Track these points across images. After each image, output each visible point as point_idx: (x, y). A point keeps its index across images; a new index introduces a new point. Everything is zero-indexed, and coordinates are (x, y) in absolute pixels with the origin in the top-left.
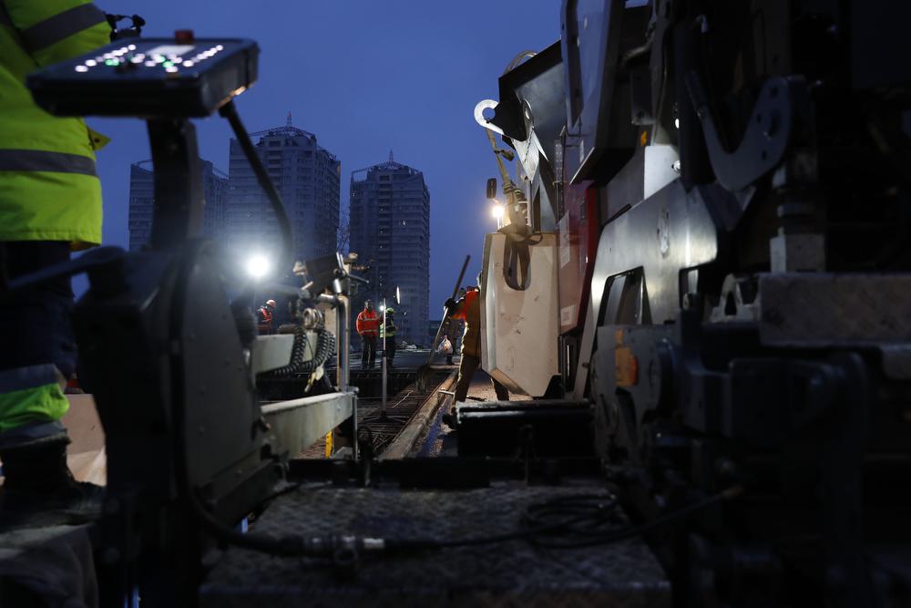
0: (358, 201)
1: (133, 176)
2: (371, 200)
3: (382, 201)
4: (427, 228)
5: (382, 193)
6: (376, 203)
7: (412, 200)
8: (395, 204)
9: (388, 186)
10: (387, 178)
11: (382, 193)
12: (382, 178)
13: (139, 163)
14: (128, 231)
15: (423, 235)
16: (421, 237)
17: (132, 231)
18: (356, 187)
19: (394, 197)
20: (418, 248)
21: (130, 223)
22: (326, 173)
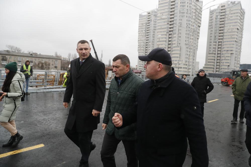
0: (211, 17)
1: (140, 17)
2: (217, 16)
3: (221, 16)
4: (243, 25)
5: (222, 13)
6: (219, 17)
7: (234, 13)
8: (227, 16)
9: (224, 9)
10: (224, 6)
11: (222, 13)
12: (222, 7)
13: (142, 13)
14: (138, 34)
15: (239, 28)
16: (238, 29)
17: (139, 34)
18: (212, 12)
19: (227, 13)
20: (237, 34)
21: (139, 31)
22: (194, 4)
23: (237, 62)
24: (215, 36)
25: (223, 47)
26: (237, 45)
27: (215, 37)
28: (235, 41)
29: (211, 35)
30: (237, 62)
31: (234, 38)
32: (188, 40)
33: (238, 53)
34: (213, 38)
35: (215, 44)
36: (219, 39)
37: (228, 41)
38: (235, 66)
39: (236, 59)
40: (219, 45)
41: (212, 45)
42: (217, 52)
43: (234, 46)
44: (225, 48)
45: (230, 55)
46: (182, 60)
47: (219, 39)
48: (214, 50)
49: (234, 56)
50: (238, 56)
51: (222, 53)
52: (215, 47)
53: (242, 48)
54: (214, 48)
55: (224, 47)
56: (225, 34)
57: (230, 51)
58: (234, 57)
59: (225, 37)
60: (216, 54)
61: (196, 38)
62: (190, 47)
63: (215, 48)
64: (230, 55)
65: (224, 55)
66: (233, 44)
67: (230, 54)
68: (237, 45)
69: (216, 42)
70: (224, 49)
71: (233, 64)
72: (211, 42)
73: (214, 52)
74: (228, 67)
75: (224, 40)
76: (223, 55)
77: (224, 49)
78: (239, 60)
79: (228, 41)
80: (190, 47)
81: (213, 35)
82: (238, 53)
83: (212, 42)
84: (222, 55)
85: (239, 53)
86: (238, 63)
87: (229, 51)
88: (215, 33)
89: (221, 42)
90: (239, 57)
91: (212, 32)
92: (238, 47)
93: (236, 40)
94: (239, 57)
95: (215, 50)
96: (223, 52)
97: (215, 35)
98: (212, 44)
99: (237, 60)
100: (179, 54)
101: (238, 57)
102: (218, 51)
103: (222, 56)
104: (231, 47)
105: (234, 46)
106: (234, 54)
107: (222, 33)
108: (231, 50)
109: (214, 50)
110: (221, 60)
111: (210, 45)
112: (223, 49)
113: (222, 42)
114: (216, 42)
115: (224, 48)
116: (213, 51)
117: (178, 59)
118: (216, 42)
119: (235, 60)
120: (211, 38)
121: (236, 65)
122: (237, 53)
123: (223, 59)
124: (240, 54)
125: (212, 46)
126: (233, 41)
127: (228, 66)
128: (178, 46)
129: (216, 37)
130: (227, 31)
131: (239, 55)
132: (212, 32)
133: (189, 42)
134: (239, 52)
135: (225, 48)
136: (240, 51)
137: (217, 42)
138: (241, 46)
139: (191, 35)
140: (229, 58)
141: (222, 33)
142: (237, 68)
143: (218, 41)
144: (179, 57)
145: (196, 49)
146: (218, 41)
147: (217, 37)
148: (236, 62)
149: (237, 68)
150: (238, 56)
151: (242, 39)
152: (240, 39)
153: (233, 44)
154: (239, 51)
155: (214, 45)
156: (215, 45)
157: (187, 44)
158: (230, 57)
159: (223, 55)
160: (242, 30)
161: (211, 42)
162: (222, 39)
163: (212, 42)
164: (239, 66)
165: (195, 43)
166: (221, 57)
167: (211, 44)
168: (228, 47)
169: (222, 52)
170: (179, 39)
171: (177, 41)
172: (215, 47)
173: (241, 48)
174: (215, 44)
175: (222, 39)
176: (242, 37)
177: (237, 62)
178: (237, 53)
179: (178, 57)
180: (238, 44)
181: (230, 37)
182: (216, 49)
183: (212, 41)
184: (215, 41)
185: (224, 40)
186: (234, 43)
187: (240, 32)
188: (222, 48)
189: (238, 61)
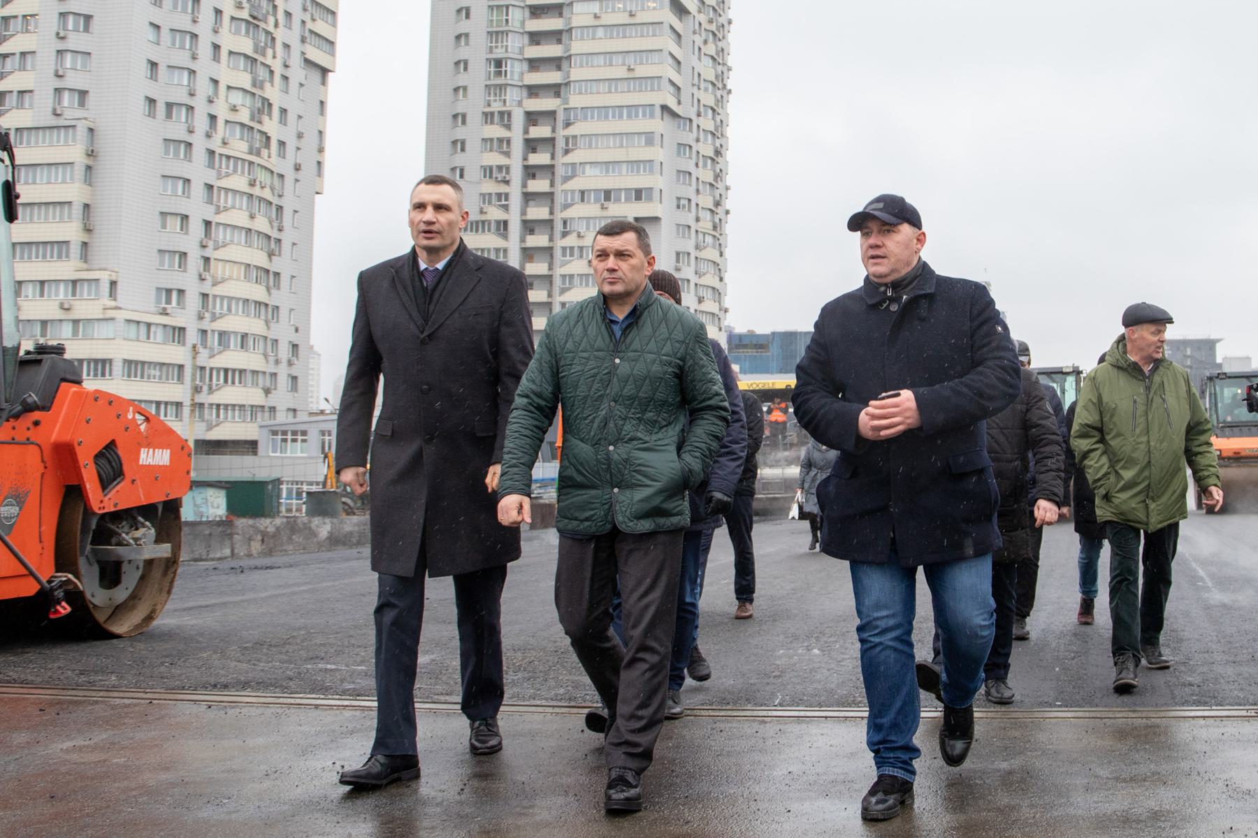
20: (673, 47)
24: (498, 63)
25: (570, 158)
26: (682, 147)
27: (499, 74)
28: (665, 108)
29: (463, 53)
31: (652, 81)
32: (183, 58)
34: (477, 77)
35: (496, 131)
36: (533, 91)
37: (604, 112)
40: (532, 145)
41: (473, 145)
42: (524, 213)
43: (657, 153)
44: (589, 170)
46: (105, 277)
47: (533, 91)
48: (491, 187)
51: (559, 216)
52: (494, 159)
54: (488, 171)
55: (573, 164)
56: (577, 47)
57: (628, 200)
59: (576, 73)
60: (515, 228)
61: (296, 60)
62: (208, 136)
63: (500, 168)
65: (579, 236)
66: (649, 138)
68: (682, 147)
69: (509, 114)
70: (576, 184)
72: (460, 118)
73: (495, 214)
75: (576, 101)
76: (571, 241)
77: (576, 184)
79: (604, 112)
80: (215, 144)
81: (477, 52)
82: (698, 220)
83: (475, 118)
84: (565, 234)
85: (706, 225)
87: (618, 200)
88: (496, 35)
89: (552, 114)
91: (464, 26)
92: (692, 169)
93: (672, 104)
95: (503, 189)
96: (568, 214)
97: (499, 53)
98: (476, 131)
100: (77, 210)
101: (702, 254)
102: (528, 197)
103: (560, 243)
104: (635, 164)
105: (657, 153)
107: (556, 36)
108: (638, 194)
109: (491, 187)
110: (557, 282)
111: (454, 142)
112: (566, 179)
113: (561, 117)
114: (505, 118)
115: (574, 171)
116: (487, 198)
117: (67, 269)
118: (501, 114)
120: (462, 79)
122: (693, 214)
123: (571, 276)
125: (476, 159)
128: (59, 128)
129: (510, 67)
130: (590, 21)
131: (709, 239)
132: (464, 26)
133: (204, 88)
135: (589, 170)
137: (518, 119)
139: (226, 18)
141: (556, 36)
143: (520, 104)
144: (75, 249)
145: (297, 168)
146: (520, 104)
147: (516, 72)
150: (697, 247)
151: (720, 101)
152: (708, 99)
153: (649, 138)
154: (706, 201)
155: (492, 140)
156: (503, 145)
157: (169, 106)
159: (571, 241)
160: (713, 27)
161: (460, 118)
162: (555, 90)
163: (475, 118)
165: (284, 111)
166: (558, 253)
167: (460, 133)
168: (607, 165)
169: (566, 207)
170: (76, 41)
171: (46, 61)
172: (494, 159)
173: (717, 177)
174: (496, 131)
175: (555, 90)
176: (719, 84)
177: (700, 300)
178: (689, 219)
179: (61, 246)
181: (621, 72)
182: (507, 182)
183: (474, 104)
184: (496, 107)
185: (576, 101)
186: (658, 125)
187: (699, 40)
188: (560, 172)
189: (708, 294)
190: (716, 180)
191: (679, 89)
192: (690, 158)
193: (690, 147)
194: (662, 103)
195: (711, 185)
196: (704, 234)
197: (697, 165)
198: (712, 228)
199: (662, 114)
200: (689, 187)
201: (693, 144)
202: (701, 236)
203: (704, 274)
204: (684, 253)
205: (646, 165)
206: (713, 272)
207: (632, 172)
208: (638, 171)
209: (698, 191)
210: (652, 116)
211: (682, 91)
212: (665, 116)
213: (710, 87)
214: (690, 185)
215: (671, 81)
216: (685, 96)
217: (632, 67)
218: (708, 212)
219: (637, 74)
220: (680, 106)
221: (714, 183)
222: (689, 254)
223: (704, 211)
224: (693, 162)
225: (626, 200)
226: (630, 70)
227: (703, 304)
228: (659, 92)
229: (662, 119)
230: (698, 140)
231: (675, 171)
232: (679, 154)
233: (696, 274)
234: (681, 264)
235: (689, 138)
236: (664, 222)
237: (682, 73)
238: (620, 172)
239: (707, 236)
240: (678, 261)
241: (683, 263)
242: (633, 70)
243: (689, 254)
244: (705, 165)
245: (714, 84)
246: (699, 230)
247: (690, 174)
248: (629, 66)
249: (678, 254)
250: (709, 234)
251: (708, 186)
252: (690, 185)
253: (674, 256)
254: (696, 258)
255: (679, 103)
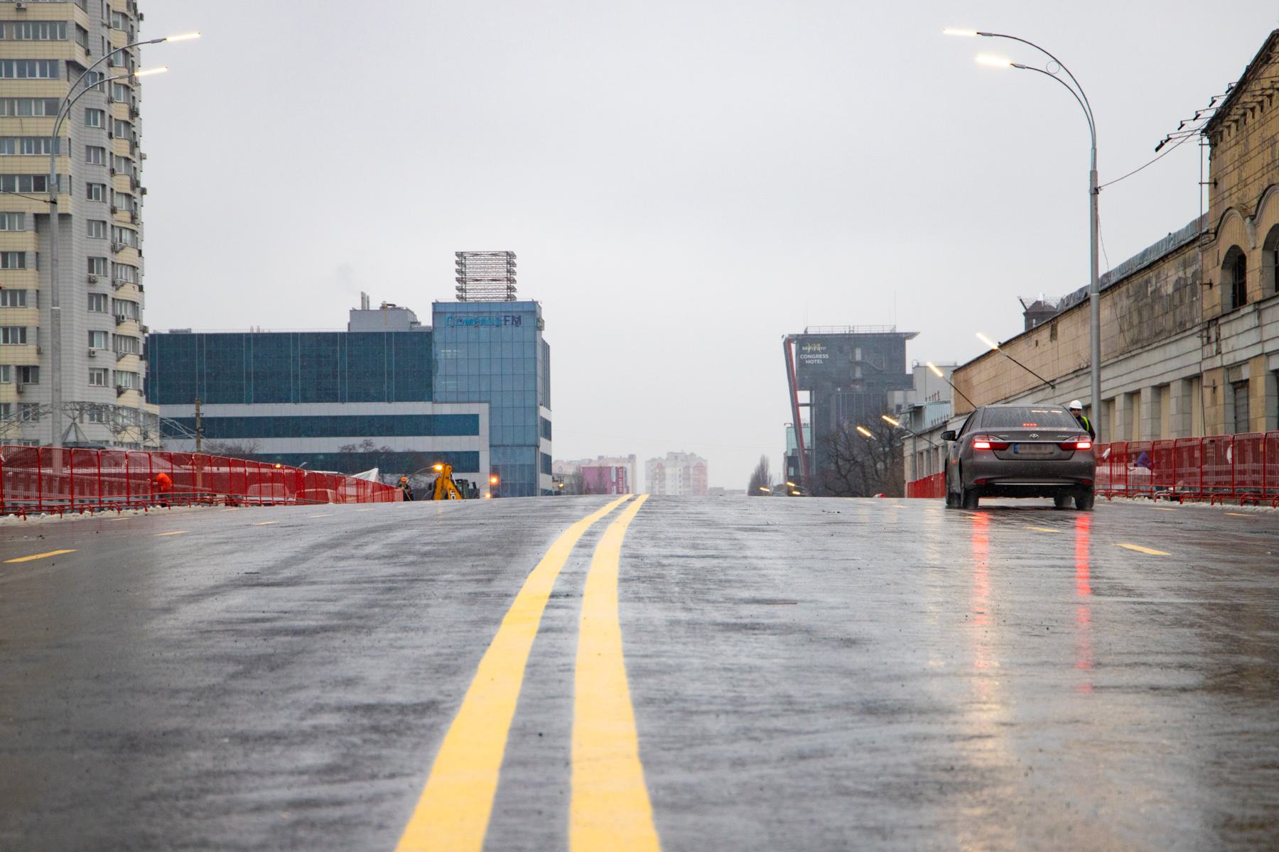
23: (110, 327)
26: (92, 114)
28: (72, 65)
30: (110, 327)
31: (54, 29)
33: (113, 211)
38: (98, 376)
39: (104, 286)
45: (24, 240)
49: (80, 245)
50: (114, 250)
53: (144, 148)
57: (24, 189)
58: (79, 269)
64: (24, 240)
67: (30, 221)
68: (92, 114)
71: (79, 343)
74: (20, 392)
78: (128, 292)
82: (113, 211)
85: (124, 216)
86: (129, 328)
90: (128, 256)
92: (105, 142)
93: (80, 58)
94: (128, 256)
99: (111, 293)
104: (33, 143)
106: (78, 227)
108: (40, 183)
119: (96, 300)
121: (106, 359)
122: (107, 207)
124: (134, 218)
126: (49, 68)
127: (27, 373)
131: (127, 236)
134: (121, 203)
136: (135, 184)
138: (136, 122)
140: (25, 279)
142: (120, 391)
148: (106, 322)
149: (120, 391)
150: (114, 250)
152: (119, 40)
153: (52, 107)
158: (30, 260)
164: (134, 363)
173: (134, 145)
177: (119, 321)
178: (102, 212)
180: (97, 99)
186: (60, 88)
189: (127, 311)
190: (132, 153)
191: (85, 32)
192: (103, 128)
193: (102, 112)
194: (68, 58)
195: (127, 159)
196: (121, 229)
197: (110, 136)
198: (129, 220)
199: (68, 71)
200: (102, 168)
201: (104, 107)
202: (117, 232)
203: (122, 286)
204: (98, 259)
205: (52, 144)
206: (132, 281)
207: (29, 151)
208: (38, 151)
209: (113, 172)
210: (54, 74)
211: (89, 34)
212: (71, 74)
213: (120, 20)
214: (104, 166)
215: (78, 27)
216: (94, 44)
217: (23, 6)
218: (124, 197)
219: (31, 16)
220: (89, 58)
221: (130, 157)
222: (105, 259)
223: (120, 197)
224: (105, 133)
225: (21, 190)
226: (19, 9)
227: (122, 326)
228: (64, 44)
229: (68, 80)
230: (110, 101)
231: (84, 147)
232: (88, 122)
233: (113, 285)
234: (95, 274)
235: (97, 99)
236: (74, 218)
237: (88, 9)
238: (12, 151)
239: (124, 231)
240: (91, 270)
241: (98, 273)
242: (25, 9)
243: (105, 259)
244: (118, 133)
245: (125, 16)
246: (116, 224)
247: (103, 149)
248: (19, 5)
249: (91, 260)
250: (127, 229)
251: (123, 161)
252: (104, 166)
253: (86, 263)
254: (113, 263)
255: (88, 53)
